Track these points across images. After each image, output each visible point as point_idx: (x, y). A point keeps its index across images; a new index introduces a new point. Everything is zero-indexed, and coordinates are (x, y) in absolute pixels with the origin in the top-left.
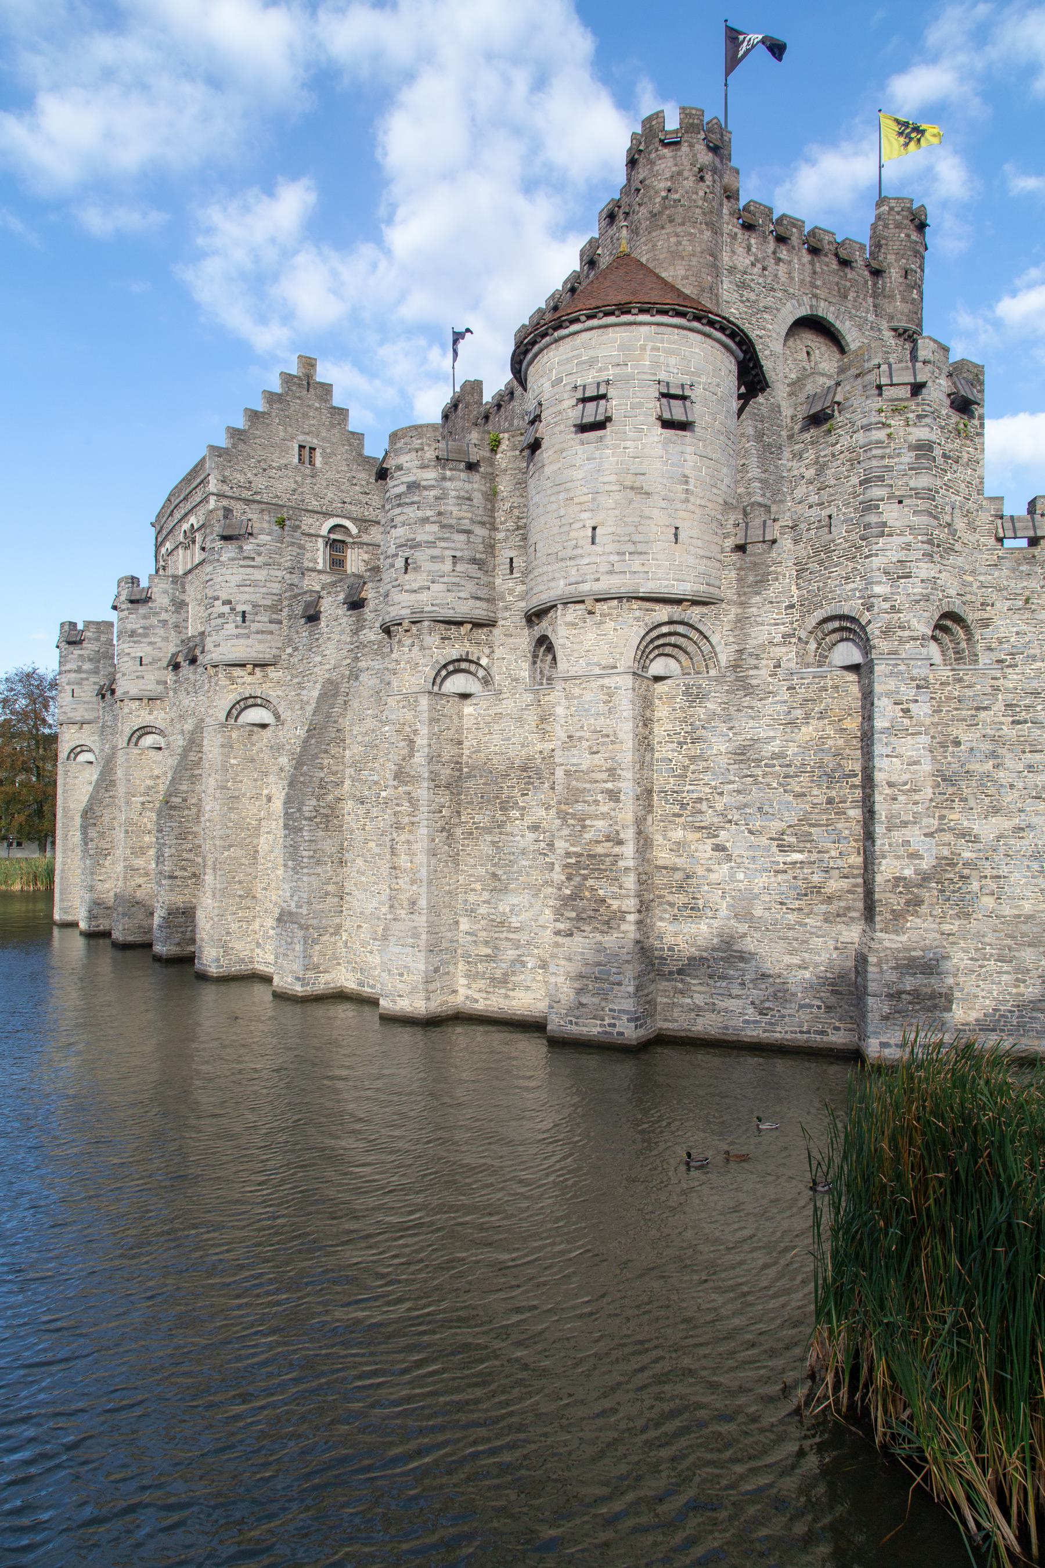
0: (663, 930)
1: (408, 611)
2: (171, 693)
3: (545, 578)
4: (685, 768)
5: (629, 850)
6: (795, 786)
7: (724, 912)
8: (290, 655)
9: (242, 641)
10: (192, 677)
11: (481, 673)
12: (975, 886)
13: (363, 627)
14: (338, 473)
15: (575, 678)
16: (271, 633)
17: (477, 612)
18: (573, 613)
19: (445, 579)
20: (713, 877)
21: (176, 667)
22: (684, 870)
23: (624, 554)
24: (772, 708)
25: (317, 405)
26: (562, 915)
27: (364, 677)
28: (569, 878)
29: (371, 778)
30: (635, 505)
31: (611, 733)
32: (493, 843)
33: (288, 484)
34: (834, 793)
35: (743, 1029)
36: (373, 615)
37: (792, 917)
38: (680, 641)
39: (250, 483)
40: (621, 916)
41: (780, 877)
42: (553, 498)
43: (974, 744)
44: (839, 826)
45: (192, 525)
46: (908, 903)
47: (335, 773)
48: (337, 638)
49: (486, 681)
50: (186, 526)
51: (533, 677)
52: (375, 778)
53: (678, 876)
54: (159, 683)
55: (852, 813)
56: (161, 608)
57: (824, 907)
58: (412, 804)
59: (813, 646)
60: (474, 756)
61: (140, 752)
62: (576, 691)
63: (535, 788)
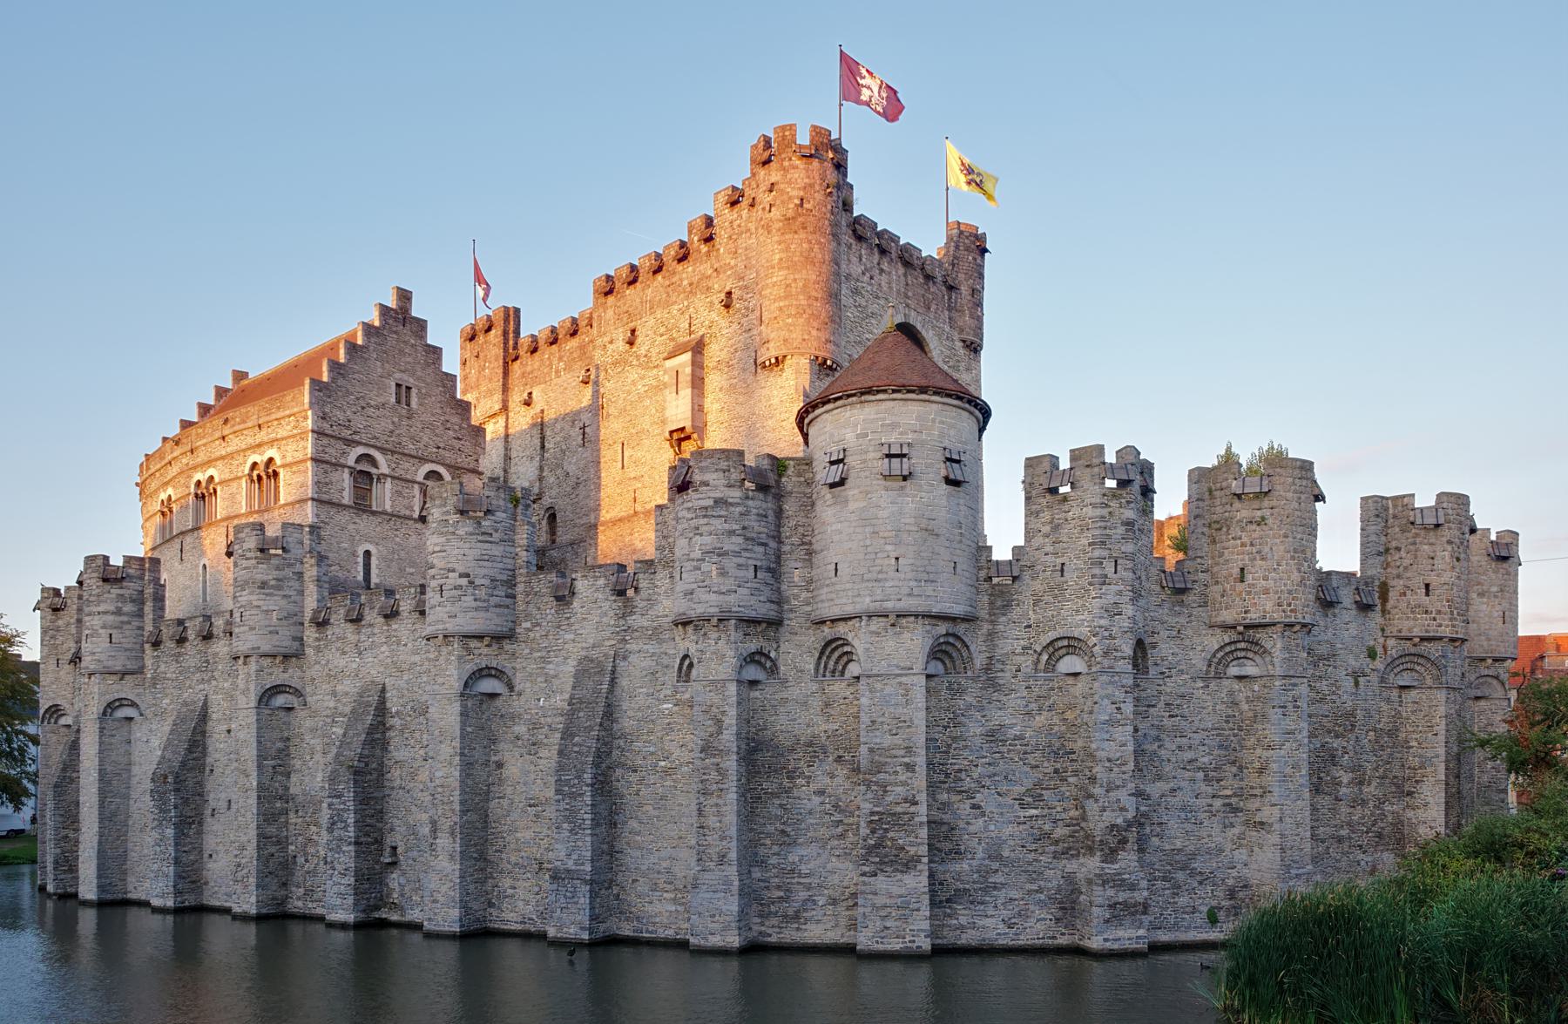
0: (934, 870)
1: (717, 610)
2: (309, 651)
3: (850, 593)
4: (949, 746)
5: (922, 809)
6: (1031, 759)
7: (980, 855)
8: (529, 630)
9: (482, 614)
10: (352, 637)
11: (768, 664)
12: (1148, 830)
13: (632, 613)
14: (433, 415)
15: (878, 676)
16: (508, 607)
17: (773, 613)
18: (876, 624)
19: (749, 585)
20: (972, 829)
21: (321, 624)
22: (949, 824)
23: (920, 581)
24: (1014, 701)
25: (413, 342)
26: (867, 860)
27: (632, 658)
28: (873, 832)
29: (647, 749)
30: (928, 543)
31: (907, 718)
32: (781, 806)
33: (386, 425)
34: (1058, 766)
35: (997, 939)
36: (645, 603)
37: (1031, 856)
38: (949, 648)
39: (349, 421)
40: (916, 860)
41: (1021, 827)
42: (858, 530)
43: (1147, 731)
44: (1063, 789)
45: (271, 460)
46: (1119, 842)
47: (605, 744)
48: (597, 619)
49: (773, 670)
50: (260, 458)
51: (817, 670)
52: (652, 749)
53: (944, 828)
54: (295, 639)
55: (1071, 780)
56: (296, 560)
57: (1053, 848)
58: (720, 774)
59: (1045, 657)
60: (760, 733)
61: (269, 712)
62: (878, 686)
63: (820, 761)
